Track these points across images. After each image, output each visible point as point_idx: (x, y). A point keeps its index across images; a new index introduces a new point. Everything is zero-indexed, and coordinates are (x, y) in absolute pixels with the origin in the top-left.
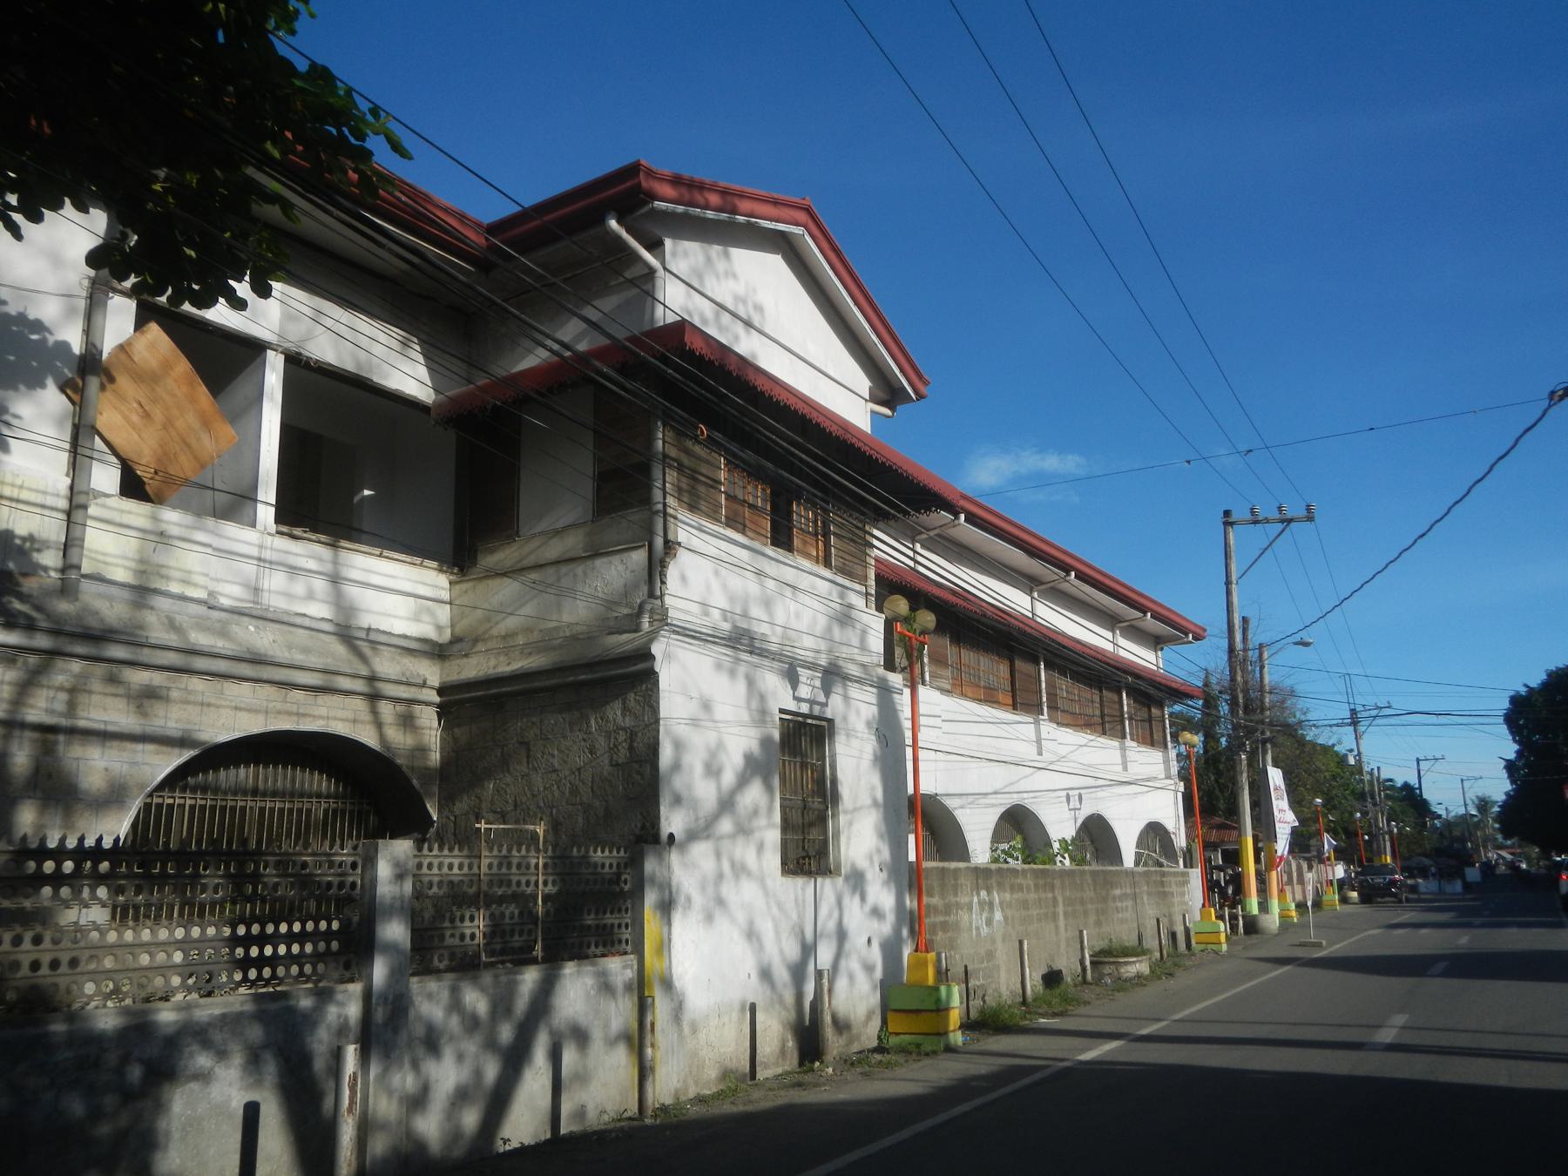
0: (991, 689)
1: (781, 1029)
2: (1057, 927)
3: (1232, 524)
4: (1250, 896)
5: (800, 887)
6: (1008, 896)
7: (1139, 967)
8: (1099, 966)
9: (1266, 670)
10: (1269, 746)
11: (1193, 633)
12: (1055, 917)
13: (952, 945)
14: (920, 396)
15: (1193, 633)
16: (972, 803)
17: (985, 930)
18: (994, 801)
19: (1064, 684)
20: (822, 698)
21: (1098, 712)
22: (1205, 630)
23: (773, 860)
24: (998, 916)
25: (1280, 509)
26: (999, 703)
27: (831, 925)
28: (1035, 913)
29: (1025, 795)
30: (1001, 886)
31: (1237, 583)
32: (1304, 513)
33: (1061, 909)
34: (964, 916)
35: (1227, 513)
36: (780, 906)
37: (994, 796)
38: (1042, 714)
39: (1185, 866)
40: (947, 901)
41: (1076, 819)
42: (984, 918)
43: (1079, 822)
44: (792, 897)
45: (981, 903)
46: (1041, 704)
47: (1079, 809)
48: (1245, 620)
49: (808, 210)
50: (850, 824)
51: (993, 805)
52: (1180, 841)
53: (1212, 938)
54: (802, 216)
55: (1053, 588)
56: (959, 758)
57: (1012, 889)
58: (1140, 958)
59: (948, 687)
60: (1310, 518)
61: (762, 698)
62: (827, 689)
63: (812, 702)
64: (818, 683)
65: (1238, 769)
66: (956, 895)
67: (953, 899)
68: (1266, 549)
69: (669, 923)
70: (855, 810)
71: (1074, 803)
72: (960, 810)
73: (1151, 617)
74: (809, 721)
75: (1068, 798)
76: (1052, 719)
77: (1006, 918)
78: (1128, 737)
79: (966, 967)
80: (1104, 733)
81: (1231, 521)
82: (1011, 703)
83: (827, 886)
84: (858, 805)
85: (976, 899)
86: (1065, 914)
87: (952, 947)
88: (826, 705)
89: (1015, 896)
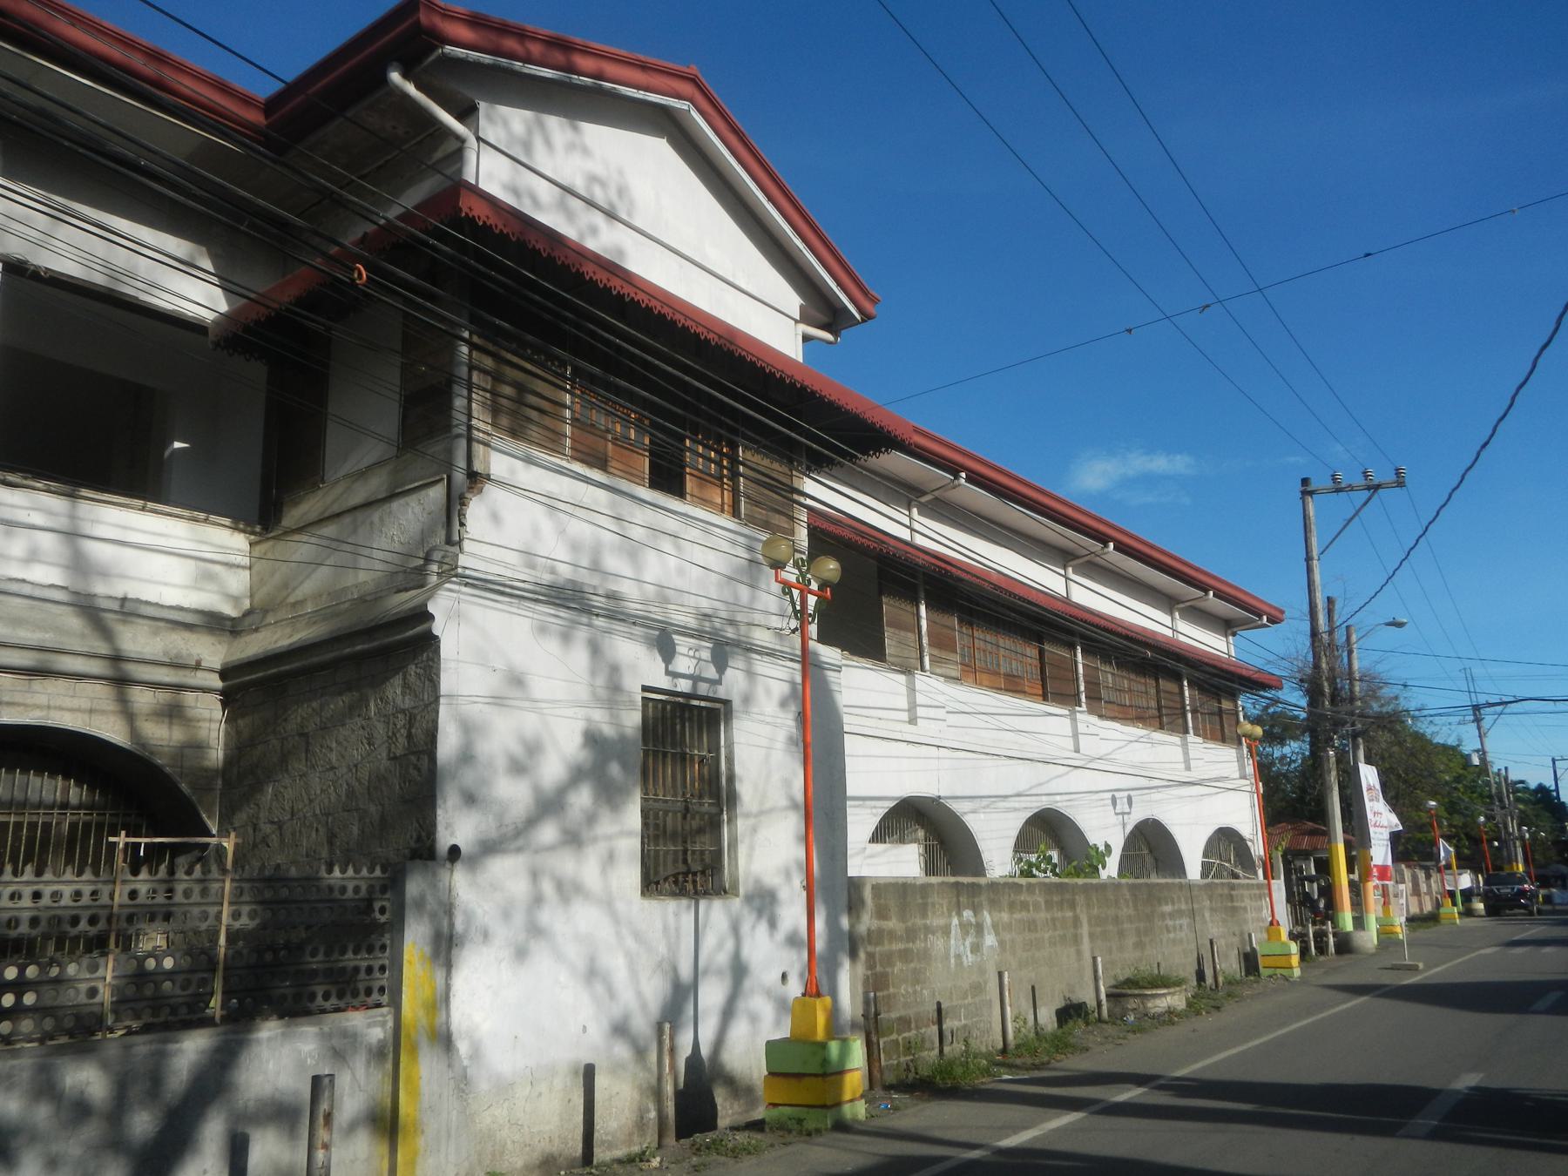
0: (1014, 676)
1: (636, 1096)
2: (1079, 953)
3: (1311, 493)
4: (1343, 910)
5: (671, 913)
6: (1005, 916)
7: (1174, 1000)
8: (1122, 999)
9: (1355, 654)
10: (1360, 740)
11: (1268, 615)
12: (1076, 940)
13: (917, 978)
14: (867, 317)
15: (1268, 615)
16: (988, 806)
17: (969, 959)
18: (1017, 805)
19: (1109, 675)
20: (711, 672)
21: (1153, 704)
22: (1282, 612)
23: (630, 875)
24: (990, 940)
25: (1365, 474)
26: (1025, 692)
27: (723, 958)
28: (1047, 936)
30: (994, 905)
31: (1319, 559)
32: (1394, 478)
33: (1085, 930)
34: (937, 943)
35: (1305, 482)
36: (638, 936)
37: (1017, 799)
38: (1080, 706)
39: (1266, 877)
40: (909, 924)
41: (1124, 825)
42: (967, 943)
43: (1129, 828)
44: (659, 925)
45: (964, 927)
46: (1078, 694)
48: (1330, 601)
49: (694, 81)
50: (754, 830)
51: (1015, 810)
52: (1258, 849)
53: (1282, 961)
54: (687, 88)
55: (1089, 562)
57: (1012, 906)
58: (1172, 990)
59: (955, 674)
60: (1400, 483)
61: (615, 670)
62: (720, 662)
63: (695, 679)
64: (706, 655)
65: (1326, 768)
66: (924, 916)
67: (919, 922)
68: (1352, 519)
69: (449, 966)
70: (761, 813)
71: (1122, 806)
72: (972, 815)
73: (1214, 595)
74: (695, 703)
75: (1114, 801)
76: (1091, 711)
77: (1002, 943)
78: (1191, 731)
79: (939, 1004)
80: (1161, 727)
81: (1309, 489)
82: (1041, 692)
83: (716, 913)
84: (768, 805)
85: (955, 921)
86: (1091, 936)
87: (917, 981)
88: (719, 682)
89: (1017, 916)
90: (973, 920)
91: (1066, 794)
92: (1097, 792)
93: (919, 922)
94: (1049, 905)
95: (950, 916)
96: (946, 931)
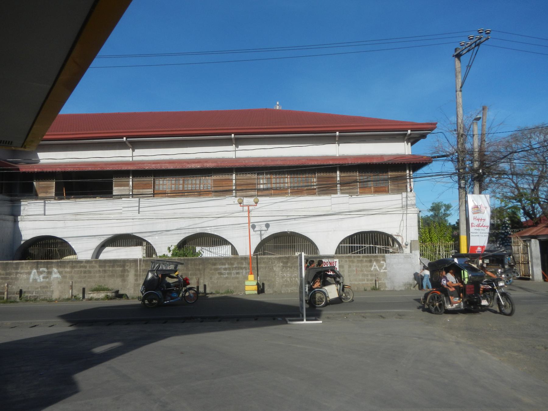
2: (124, 280)
6: (68, 270)
16: (159, 234)
18: (179, 232)
29: (208, 228)
40: (8, 271)
41: (261, 235)
45: (40, 273)
51: (178, 234)
77: (64, 277)
93: (13, 271)
94: (100, 266)
96: (29, 273)
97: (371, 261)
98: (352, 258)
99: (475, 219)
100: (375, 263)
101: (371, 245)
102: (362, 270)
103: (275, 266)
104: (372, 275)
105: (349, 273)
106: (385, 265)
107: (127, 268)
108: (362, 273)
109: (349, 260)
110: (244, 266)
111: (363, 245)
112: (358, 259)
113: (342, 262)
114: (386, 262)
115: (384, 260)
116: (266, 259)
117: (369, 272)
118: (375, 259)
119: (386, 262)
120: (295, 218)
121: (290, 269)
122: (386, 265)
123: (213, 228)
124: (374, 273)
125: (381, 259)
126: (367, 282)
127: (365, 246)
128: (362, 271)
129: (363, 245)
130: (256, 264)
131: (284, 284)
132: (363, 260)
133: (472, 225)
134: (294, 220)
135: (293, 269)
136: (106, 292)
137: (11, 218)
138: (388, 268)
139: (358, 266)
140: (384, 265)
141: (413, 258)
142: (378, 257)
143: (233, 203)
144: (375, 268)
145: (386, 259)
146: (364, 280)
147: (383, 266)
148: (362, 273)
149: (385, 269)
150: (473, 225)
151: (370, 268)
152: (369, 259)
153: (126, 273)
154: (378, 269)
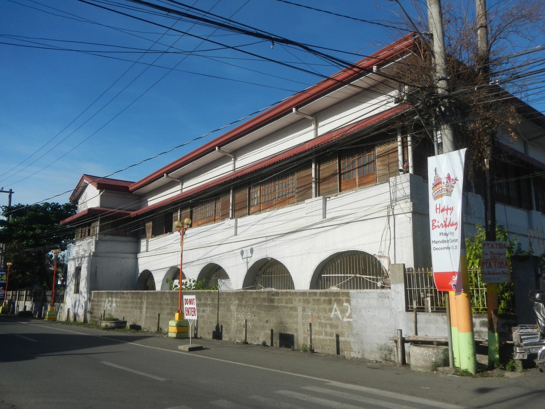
2: (141, 312)
5: (75, 295)
6: (119, 300)
12: (141, 308)
13: (98, 310)
17: (109, 308)
18: (199, 263)
24: (114, 305)
28: (130, 306)
30: (116, 297)
33: (145, 306)
34: (103, 304)
41: (247, 263)
42: (109, 304)
45: (109, 301)
47: (252, 257)
56: (172, 254)
57: (121, 298)
66: (101, 298)
67: (100, 299)
71: (247, 254)
75: (242, 253)
77: (117, 306)
85: (107, 300)
86: (147, 308)
87: (98, 310)
89: (122, 300)
90: (111, 300)
91: (217, 255)
92: (233, 251)
94: (132, 298)
95: (106, 299)
96: (105, 302)
97: (330, 302)
98: (308, 295)
99: (438, 210)
100: (335, 306)
101: (358, 275)
102: (318, 316)
103: (232, 303)
104: (332, 326)
105: (303, 319)
106: (349, 310)
107: (143, 300)
108: (319, 321)
109: (303, 299)
110: (209, 302)
111: (349, 275)
112: (314, 298)
113: (296, 302)
114: (350, 304)
115: (348, 301)
116: (225, 294)
117: (328, 320)
118: (335, 298)
119: (350, 304)
120: (272, 239)
121: (244, 309)
122: (351, 309)
123: (217, 256)
124: (334, 322)
125: (344, 298)
126: (325, 338)
127: (350, 277)
128: (319, 318)
129: (349, 275)
130: (217, 301)
131: (238, 329)
132: (320, 299)
133: (433, 225)
134: (272, 241)
135: (247, 309)
136: (106, 321)
137: (132, 256)
138: (354, 316)
139: (314, 310)
140: (348, 310)
141: (393, 299)
142: (339, 296)
143: (228, 226)
144: (335, 314)
145: (352, 299)
146: (321, 334)
147: (347, 312)
148: (319, 321)
149: (350, 317)
150: (436, 224)
151: (330, 313)
152: (327, 298)
153: (142, 306)
154: (340, 316)
